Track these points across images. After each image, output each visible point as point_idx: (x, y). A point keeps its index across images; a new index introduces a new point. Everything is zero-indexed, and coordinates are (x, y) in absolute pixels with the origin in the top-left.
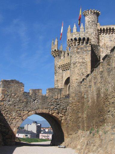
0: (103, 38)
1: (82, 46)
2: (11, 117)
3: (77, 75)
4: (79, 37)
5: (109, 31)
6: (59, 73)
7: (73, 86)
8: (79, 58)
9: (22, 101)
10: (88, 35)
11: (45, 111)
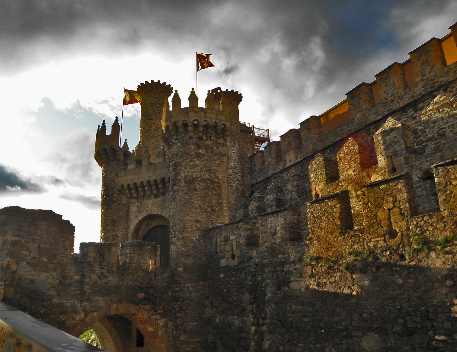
1: (209, 142)
3: (198, 210)
4: (205, 119)
6: (119, 204)
7: (188, 237)
8: (202, 169)
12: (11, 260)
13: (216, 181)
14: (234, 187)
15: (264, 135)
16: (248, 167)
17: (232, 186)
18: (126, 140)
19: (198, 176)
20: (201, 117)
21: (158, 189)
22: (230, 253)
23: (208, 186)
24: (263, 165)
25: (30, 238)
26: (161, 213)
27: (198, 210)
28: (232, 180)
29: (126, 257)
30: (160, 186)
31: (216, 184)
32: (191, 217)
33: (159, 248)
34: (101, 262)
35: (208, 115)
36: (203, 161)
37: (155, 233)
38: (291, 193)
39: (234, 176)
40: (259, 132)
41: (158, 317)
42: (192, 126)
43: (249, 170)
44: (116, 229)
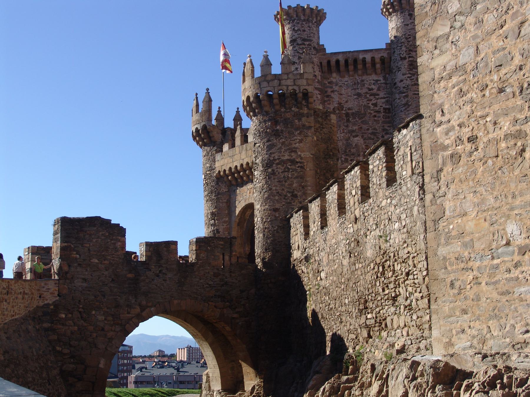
0: (336, 88)
4: (280, 88)
5: (351, 68)
6: (219, 194)
8: (281, 148)
10: (304, 82)
13: (298, 160)
19: (276, 157)
20: (274, 87)
23: (288, 168)
27: (277, 198)
31: (299, 164)
35: (283, 82)
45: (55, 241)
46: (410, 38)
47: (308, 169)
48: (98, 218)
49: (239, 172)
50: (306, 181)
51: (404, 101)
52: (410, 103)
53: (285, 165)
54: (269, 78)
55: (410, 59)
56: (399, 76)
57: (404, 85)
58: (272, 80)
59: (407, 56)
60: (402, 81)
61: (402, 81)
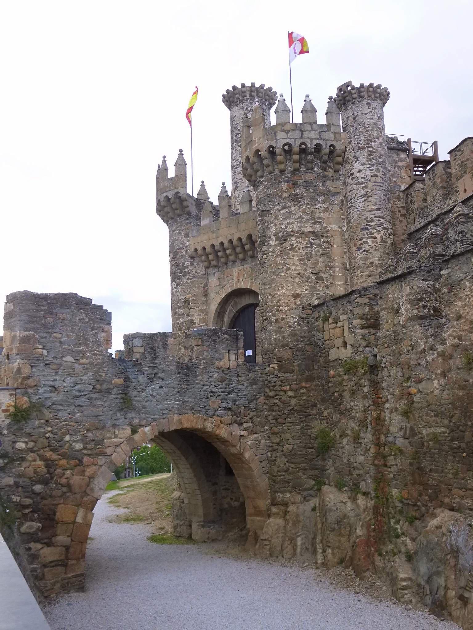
2: (63, 462)
3: (297, 280)
4: (302, 141)
6: (194, 276)
7: (283, 319)
8: (301, 217)
9: (105, 387)
11: (190, 421)
12: (22, 361)
14: (379, 239)
15: (430, 153)
16: (402, 207)
17: (376, 238)
18: (203, 182)
19: (296, 229)
21: (244, 251)
22: (341, 340)
24: (425, 201)
25: (46, 332)
26: (251, 285)
27: (297, 280)
28: (375, 228)
29: (192, 351)
30: (247, 247)
31: (324, 239)
32: (287, 290)
33: (243, 338)
34: (153, 359)
35: (306, 134)
36: (301, 205)
37: (242, 314)
38: (454, 244)
39: (377, 222)
40: (421, 149)
41: (243, 433)
42: (283, 153)
43: (405, 211)
44: (192, 312)
45: (8, 326)
46: (369, 127)
47: (335, 246)
48: (73, 296)
49: (225, 250)
50: (334, 260)
51: (363, 192)
52: (369, 195)
53: (307, 239)
54: (288, 127)
55: (369, 149)
56: (357, 166)
57: (363, 176)
58: (292, 130)
59: (366, 146)
60: (360, 171)
61: (360, 171)
